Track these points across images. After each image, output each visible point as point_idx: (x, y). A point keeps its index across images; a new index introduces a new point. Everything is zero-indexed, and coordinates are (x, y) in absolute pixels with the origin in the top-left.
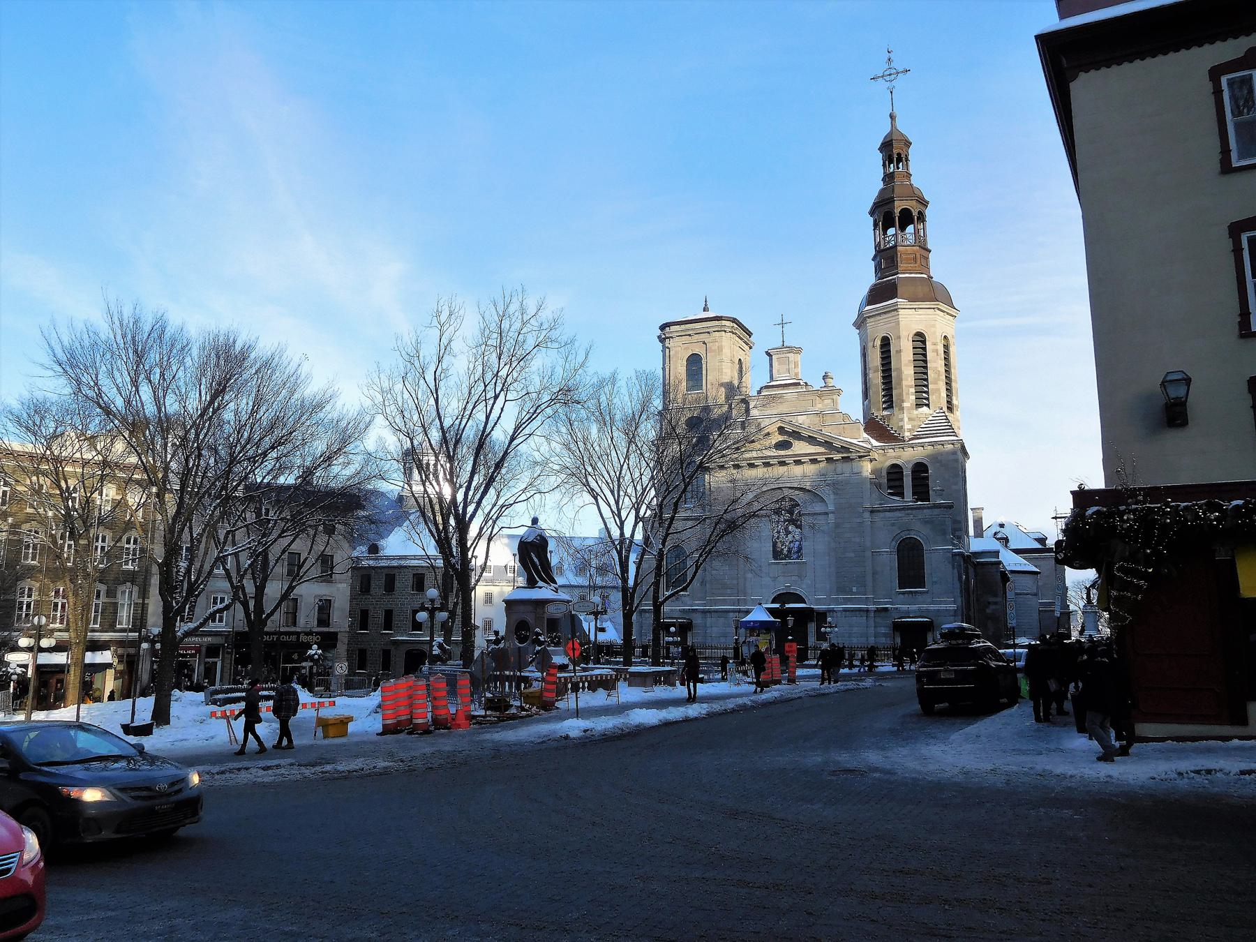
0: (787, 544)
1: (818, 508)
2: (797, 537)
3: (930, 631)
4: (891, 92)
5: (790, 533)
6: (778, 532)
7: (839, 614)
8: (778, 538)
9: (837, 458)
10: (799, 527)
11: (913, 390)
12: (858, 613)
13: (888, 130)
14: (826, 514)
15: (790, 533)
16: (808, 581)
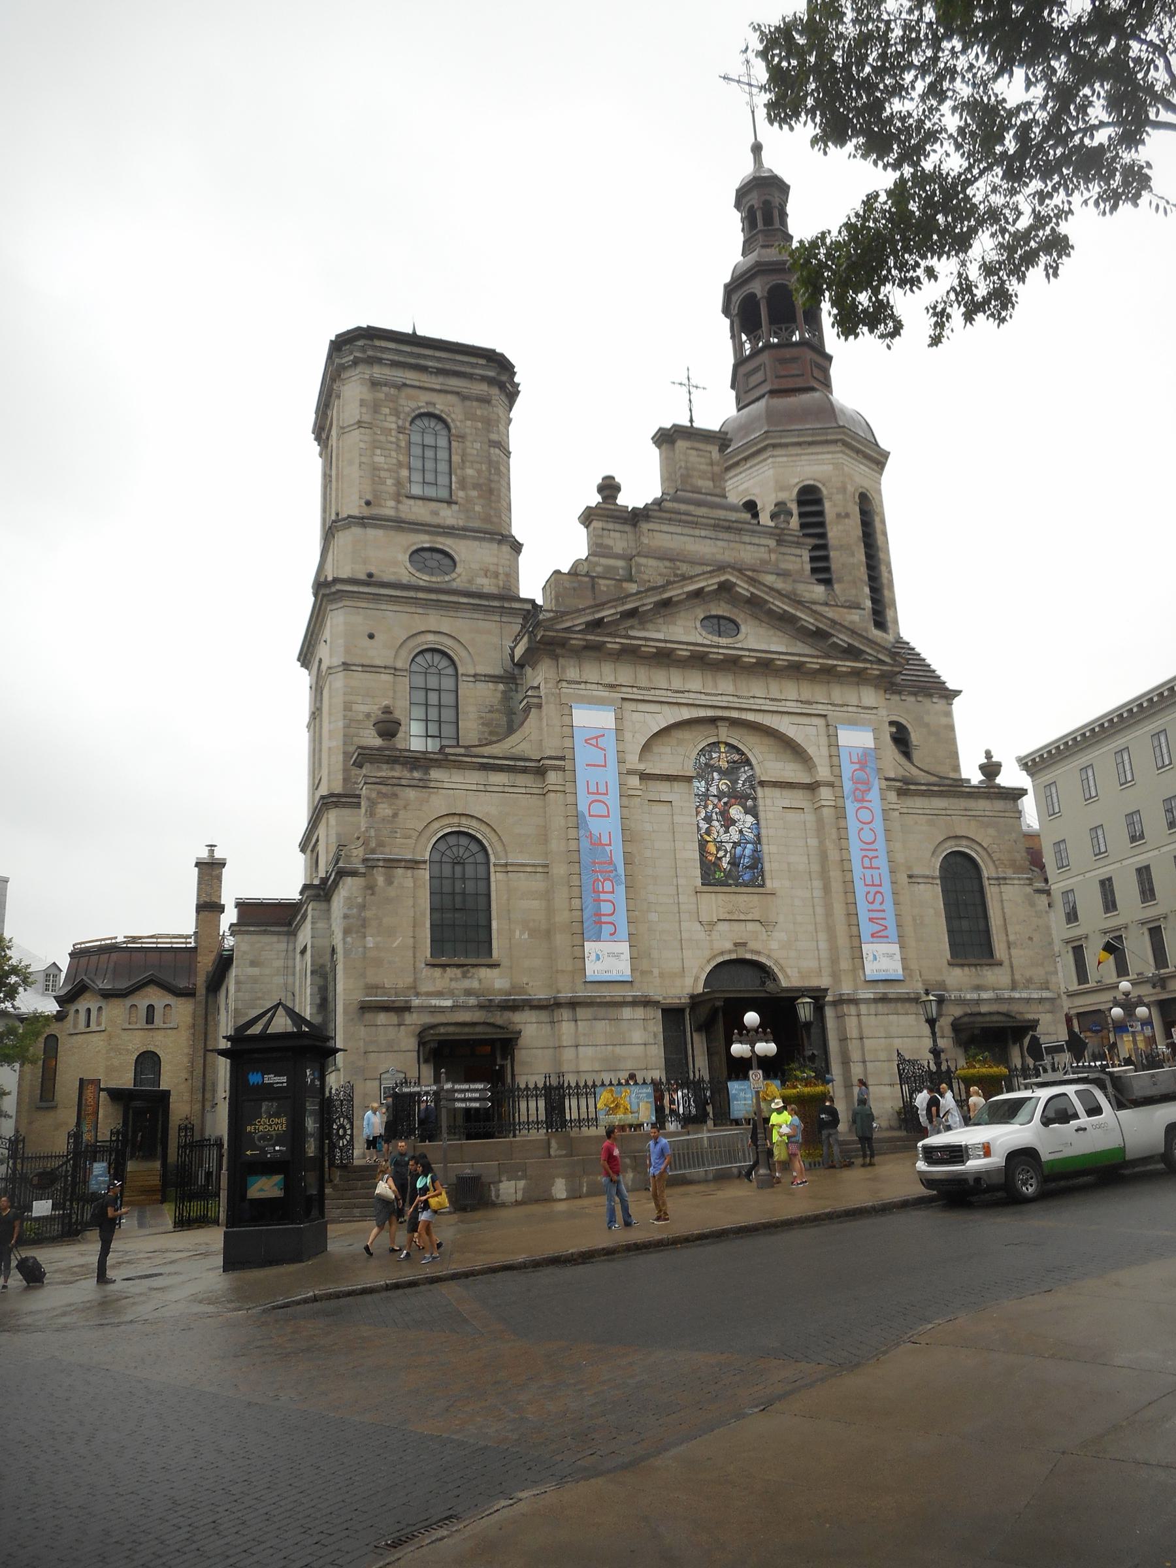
0: (729, 847)
1: (790, 771)
2: (750, 836)
3: (1014, 1043)
4: (753, 112)
5: (733, 822)
6: (708, 819)
7: (863, 1008)
8: (708, 832)
9: (844, 669)
10: (753, 812)
11: (867, 590)
12: (899, 1005)
13: (745, 169)
14: (812, 787)
15: (733, 822)
16: (780, 935)
